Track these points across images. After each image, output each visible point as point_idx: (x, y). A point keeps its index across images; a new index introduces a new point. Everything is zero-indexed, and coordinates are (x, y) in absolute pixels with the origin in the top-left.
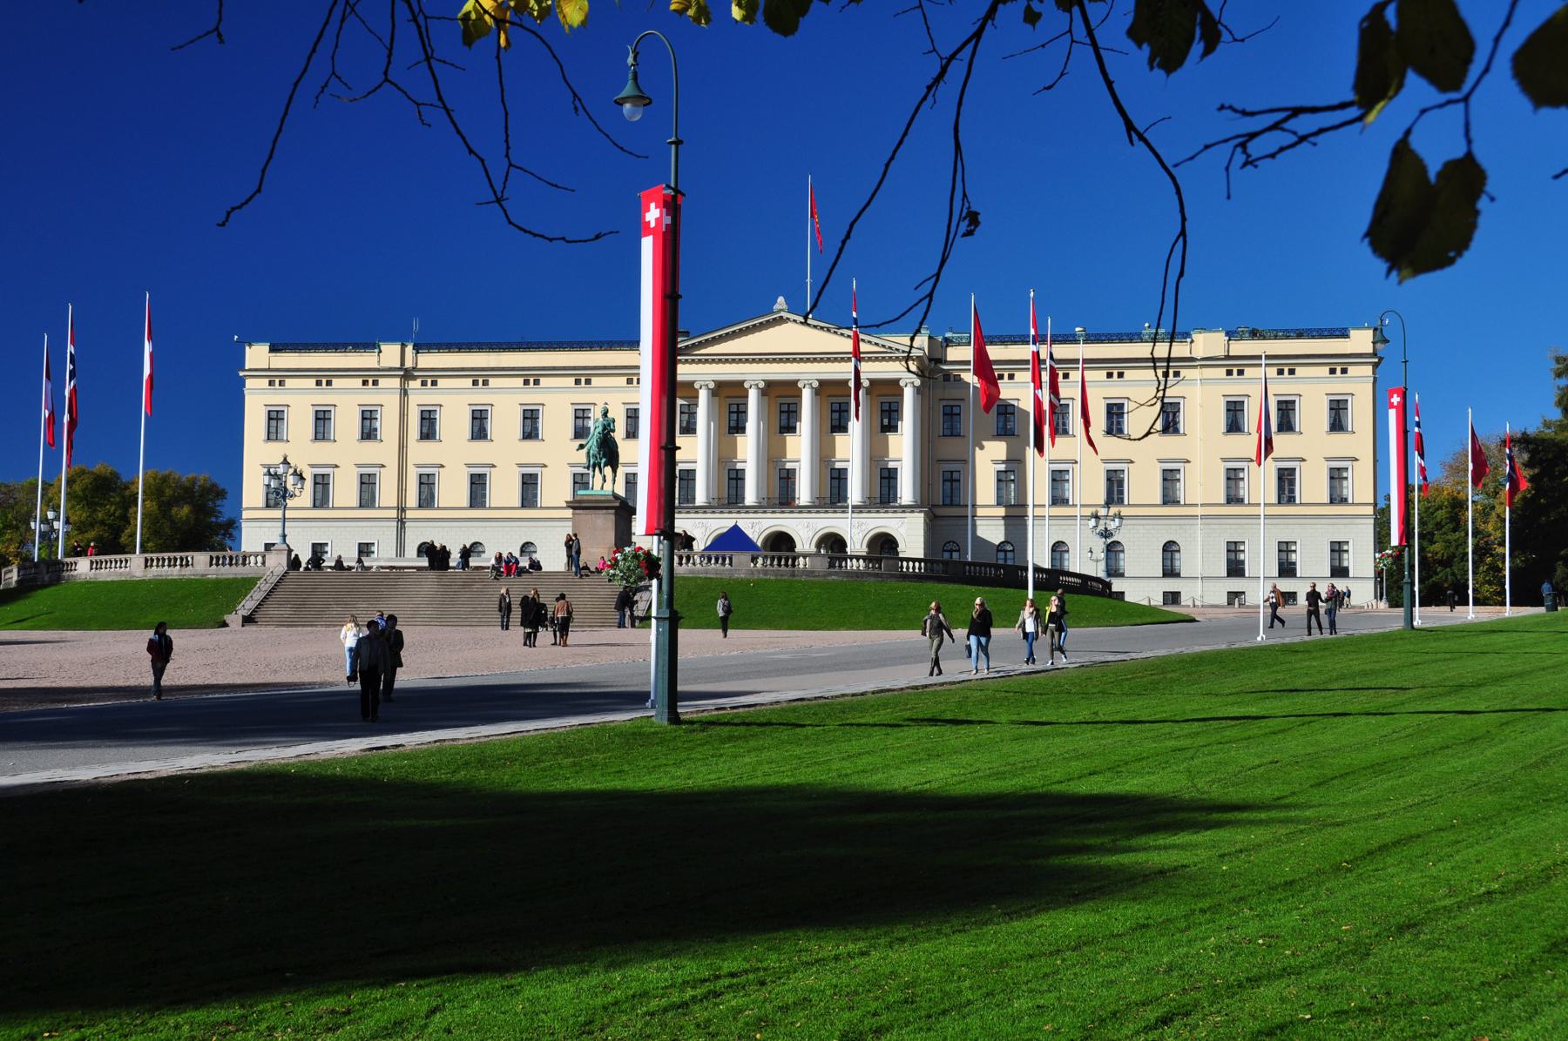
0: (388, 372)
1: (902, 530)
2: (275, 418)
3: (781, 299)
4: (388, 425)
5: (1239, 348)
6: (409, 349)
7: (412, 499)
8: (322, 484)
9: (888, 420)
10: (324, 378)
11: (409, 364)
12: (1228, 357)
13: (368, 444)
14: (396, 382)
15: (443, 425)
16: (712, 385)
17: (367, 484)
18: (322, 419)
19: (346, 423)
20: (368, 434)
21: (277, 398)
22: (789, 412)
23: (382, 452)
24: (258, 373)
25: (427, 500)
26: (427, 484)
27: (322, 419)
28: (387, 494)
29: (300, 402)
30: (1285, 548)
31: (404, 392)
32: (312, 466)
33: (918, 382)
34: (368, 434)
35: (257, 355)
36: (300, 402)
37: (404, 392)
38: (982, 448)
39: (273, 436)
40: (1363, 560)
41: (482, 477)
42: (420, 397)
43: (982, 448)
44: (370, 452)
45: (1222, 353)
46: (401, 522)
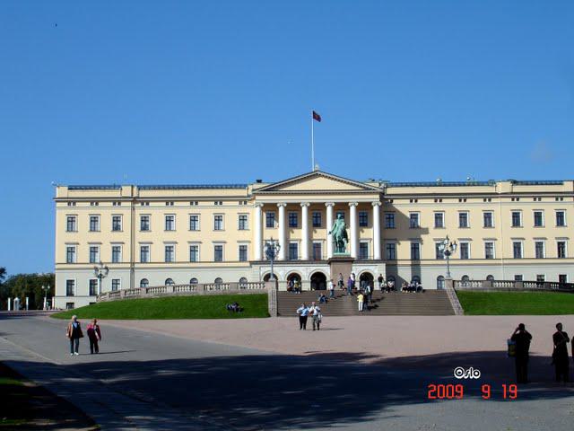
0: (126, 199)
2: (71, 220)
4: (125, 223)
5: (517, 189)
6: (135, 189)
8: (464, 248)
9: (364, 222)
11: (135, 195)
12: (512, 193)
13: (116, 234)
14: (129, 204)
15: (152, 223)
16: (309, 205)
17: (116, 251)
18: (94, 220)
20: (116, 228)
22: (293, 217)
23: (123, 236)
25: (143, 260)
26: (144, 250)
27: (94, 220)
28: (125, 255)
29: (83, 213)
31: (133, 209)
32: (460, 239)
33: (380, 204)
34: (116, 228)
35: (62, 192)
37: (133, 209)
38: (363, 232)
41: (563, 243)
42: (141, 210)
43: (363, 232)
44: (117, 237)
45: (509, 191)
46: (133, 269)
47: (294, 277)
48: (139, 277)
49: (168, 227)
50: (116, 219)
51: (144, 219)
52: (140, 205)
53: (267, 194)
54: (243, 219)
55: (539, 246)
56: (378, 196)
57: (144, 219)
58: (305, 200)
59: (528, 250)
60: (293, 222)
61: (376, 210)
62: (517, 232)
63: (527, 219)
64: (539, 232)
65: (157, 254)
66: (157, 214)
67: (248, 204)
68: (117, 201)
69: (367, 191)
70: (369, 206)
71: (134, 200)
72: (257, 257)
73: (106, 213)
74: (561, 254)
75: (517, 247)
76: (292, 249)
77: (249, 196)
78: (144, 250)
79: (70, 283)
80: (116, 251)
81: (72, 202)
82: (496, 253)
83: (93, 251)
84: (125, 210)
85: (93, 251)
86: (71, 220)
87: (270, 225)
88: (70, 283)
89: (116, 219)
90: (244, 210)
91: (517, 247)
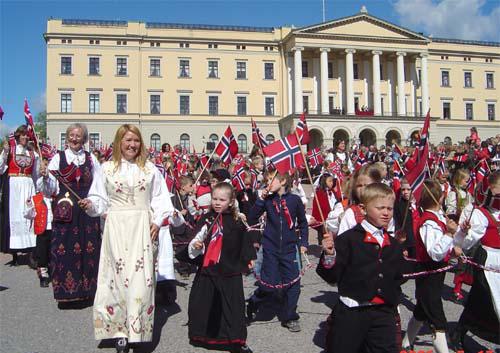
2: (66, 62)
3: (364, 8)
6: (144, 25)
7: (147, 108)
10: (94, 40)
14: (137, 44)
17: (122, 99)
18: (94, 63)
19: (108, 65)
21: (66, 50)
24: (55, 36)
25: (155, 111)
26: (155, 99)
27: (94, 63)
35: (54, 26)
36: (81, 55)
44: (122, 82)
50: (122, 61)
53: (309, 37)
57: (155, 62)
58: (350, 47)
66: (170, 57)
68: (122, 40)
69: (413, 38)
71: (142, 40)
73: (108, 55)
74: (491, 118)
78: (155, 99)
81: (67, 39)
83: (94, 97)
84: (131, 51)
85: (94, 97)
86: (66, 62)
89: (122, 61)
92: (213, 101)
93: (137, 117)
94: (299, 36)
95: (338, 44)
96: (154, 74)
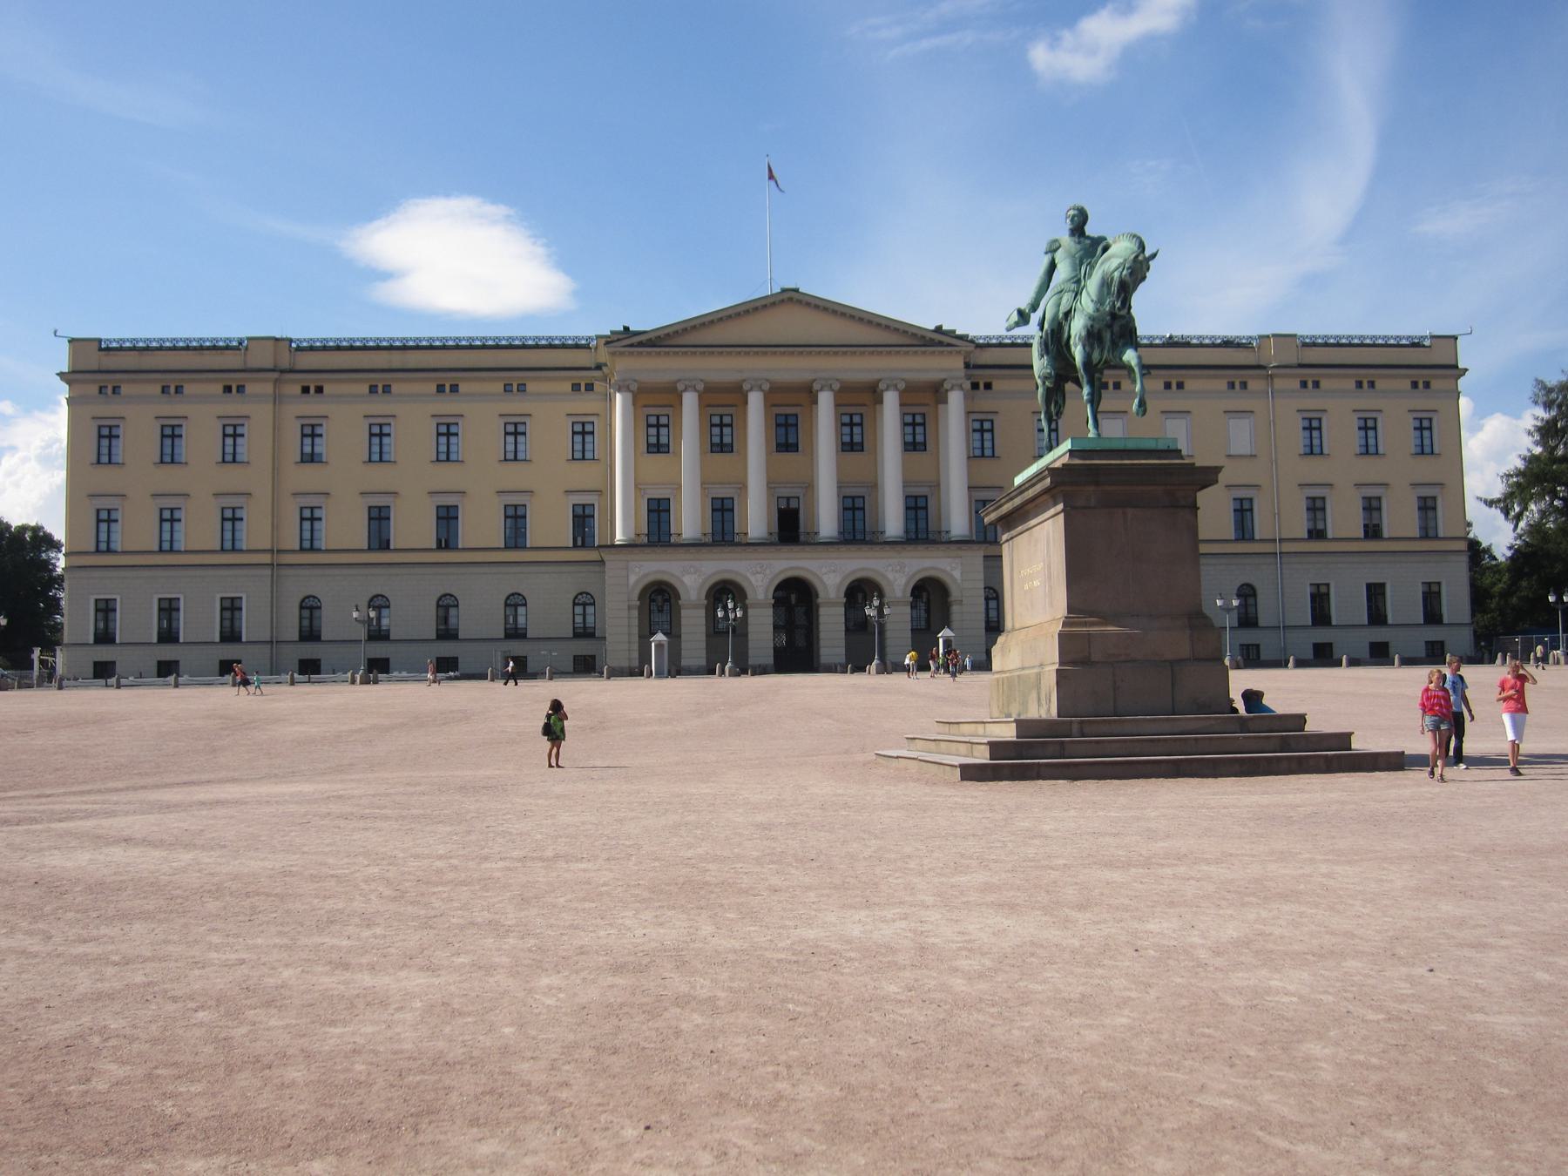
1: (957, 574)
4: (255, 444)
11: (285, 364)
14: (268, 388)
18: (171, 434)
19: (201, 439)
20: (231, 459)
23: (254, 477)
26: (310, 518)
27: (171, 434)
28: (255, 532)
30: (1375, 593)
31: (277, 399)
33: (967, 385)
39: (105, 459)
40: (1456, 602)
44: (232, 478)
45: (1294, 361)
47: (724, 591)
48: (297, 587)
49: (379, 457)
50: (232, 432)
51: (311, 432)
52: (298, 389)
54: (583, 432)
55: (1372, 506)
56: (959, 363)
57: (311, 432)
59: (1345, 519)
60: (722, 440)
61: (955, 400)
62: (1315, 470)
63: (1341, 433)
64: (1371, 470)
65: (345, 527)
67: (598, 386)
70: (937, 392)
72: (619, 537)
75: (1316, 507)
76: (723, 510)
77: (599, 367)
79: (105, 609)
80: (231, 518)
82: (1262, 525)
83: (169, 518)
85: (169, 518)
87: (657, 448)
88: (105, 609)
89: (232, 432)
90: (585, 404)
91: (1316, 507)
92: (447, 517)
93: (266, 558)
94: (622, 354)
95: (722, 369)
96: (311, 458)
